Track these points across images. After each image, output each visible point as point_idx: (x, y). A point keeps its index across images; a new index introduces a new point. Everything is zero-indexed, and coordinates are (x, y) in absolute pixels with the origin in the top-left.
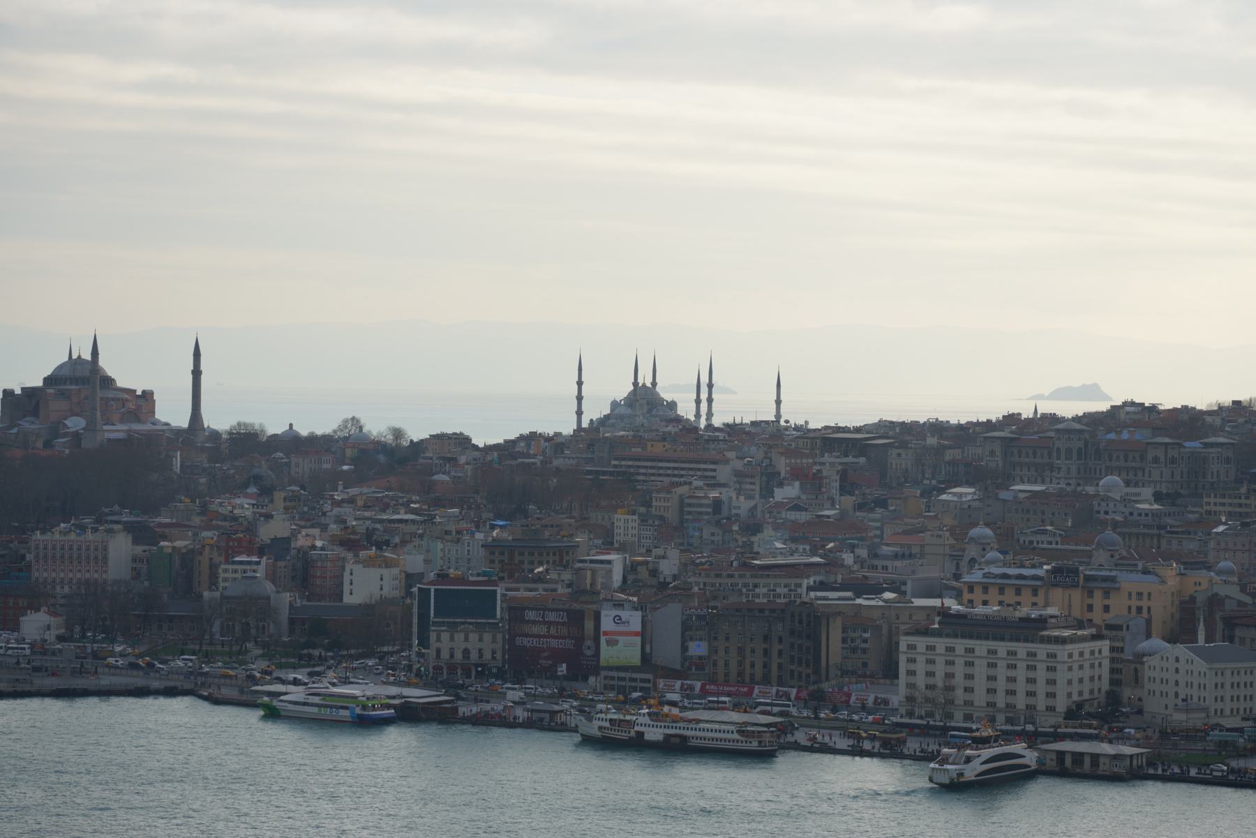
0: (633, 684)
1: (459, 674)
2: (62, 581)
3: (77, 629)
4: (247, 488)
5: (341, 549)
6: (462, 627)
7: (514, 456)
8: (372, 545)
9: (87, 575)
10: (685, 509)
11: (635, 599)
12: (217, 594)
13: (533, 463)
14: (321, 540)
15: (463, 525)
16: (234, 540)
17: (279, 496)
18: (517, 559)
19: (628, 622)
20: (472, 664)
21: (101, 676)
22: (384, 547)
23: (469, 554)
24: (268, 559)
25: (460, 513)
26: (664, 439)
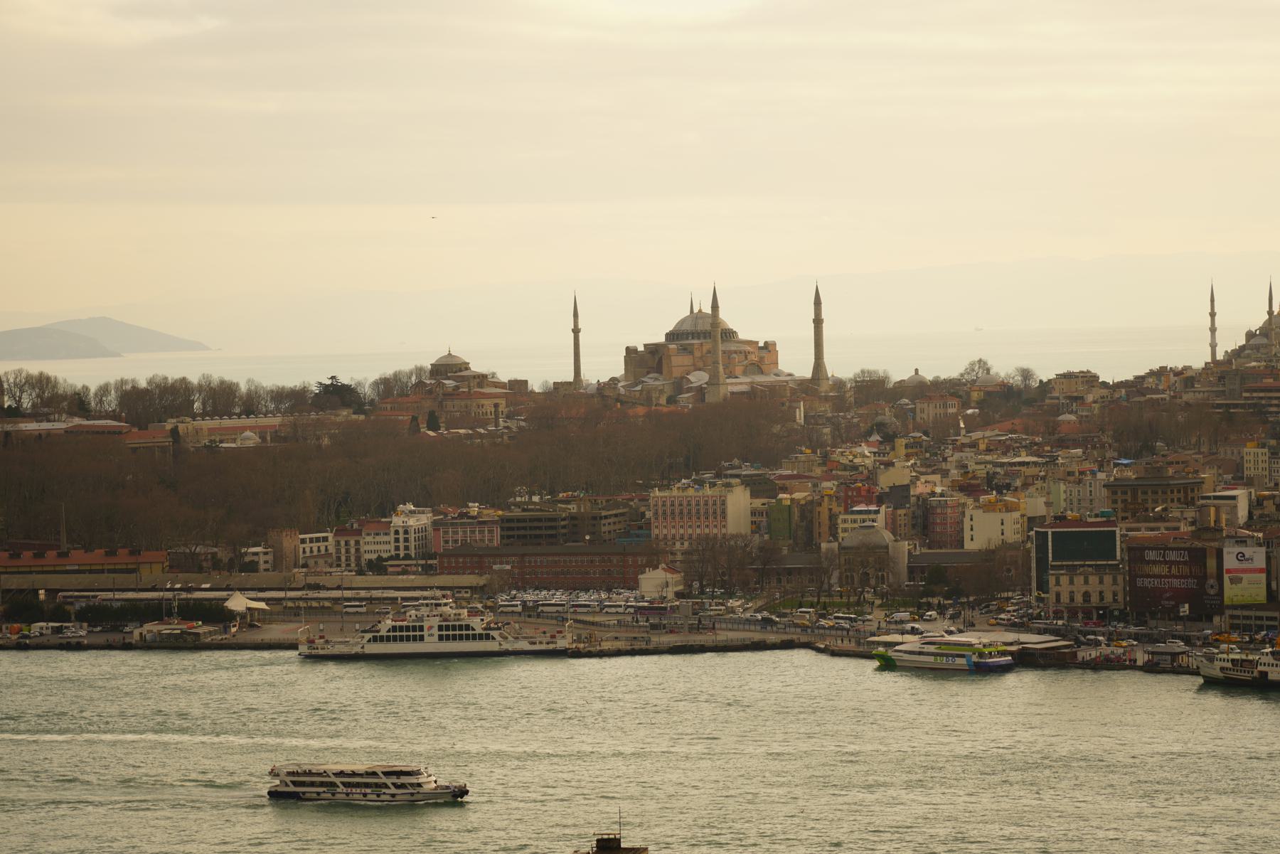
0: (1259, 622)
1: (1080, 617)
2: (682, 538)
3: (696, 584)
4: (870, 436)
5: (961, 494)
6: (1082, 569)
7: (1142, 393)
8: (992, 490)
9: (707, 531)
11: (1261, 535)
12: (836, 544)
13: (1162, 399)
14: (942, 486)
15: (1087, 465)
16: (853, 490)
17: (901, 443)
18: (1140, 497)
19: (1252, 559)
20: (1094, 607)
21: (718, 632)
22: (1005, 491)
23: (1091, 495)
24: (888, 507)
25: (1084, 453)
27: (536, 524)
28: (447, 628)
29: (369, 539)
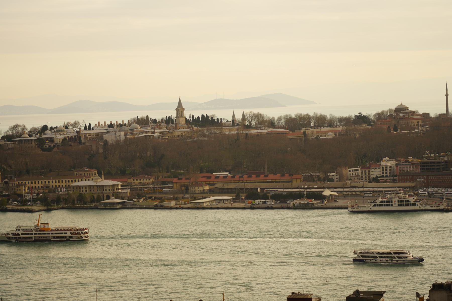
27: (433, 164)
28: (401, 201)
29: (373, 170)
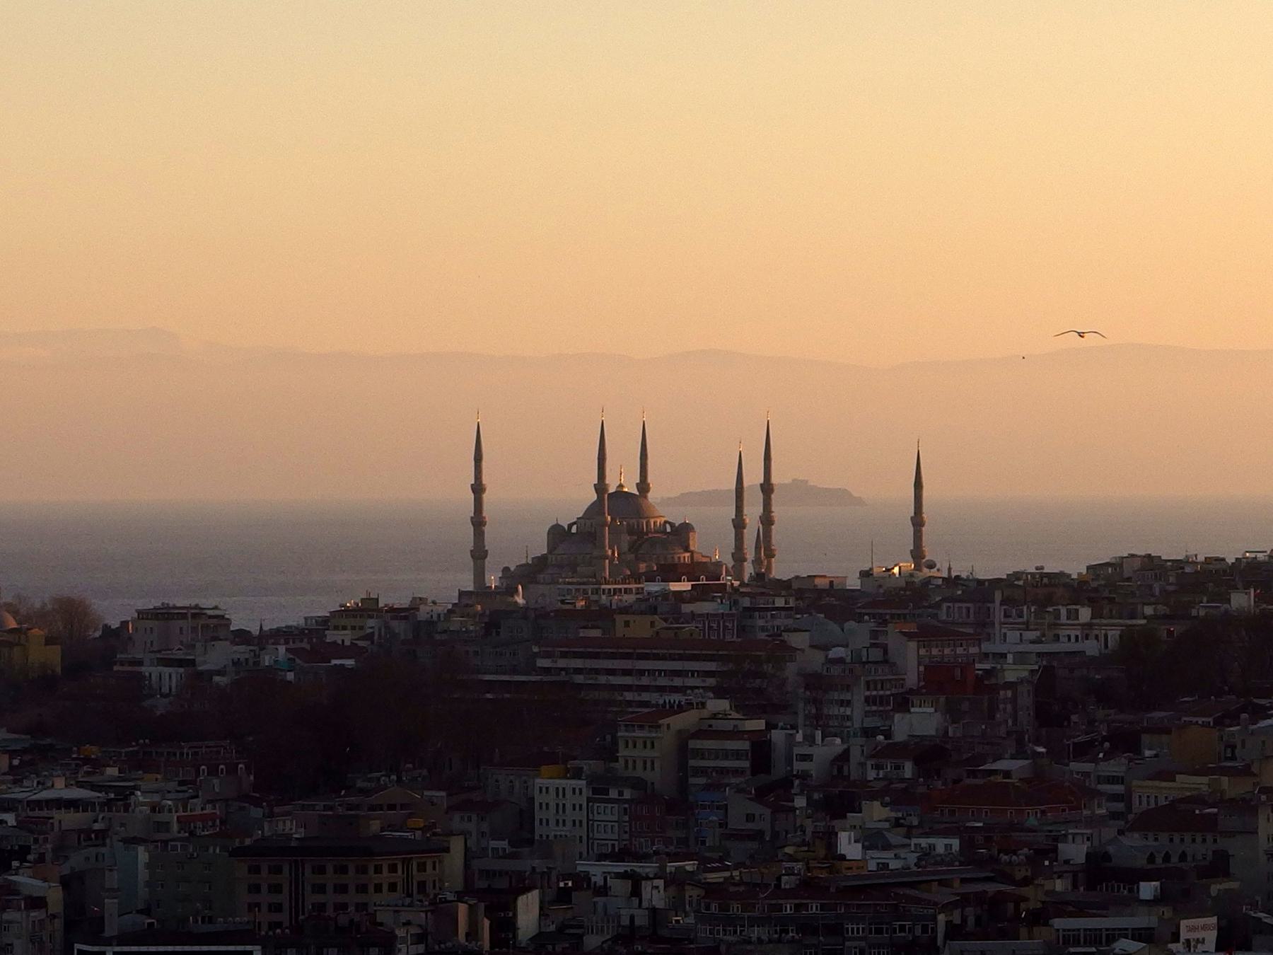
10: (692, 763)
22: (15, 864)
26: (653, 610)
